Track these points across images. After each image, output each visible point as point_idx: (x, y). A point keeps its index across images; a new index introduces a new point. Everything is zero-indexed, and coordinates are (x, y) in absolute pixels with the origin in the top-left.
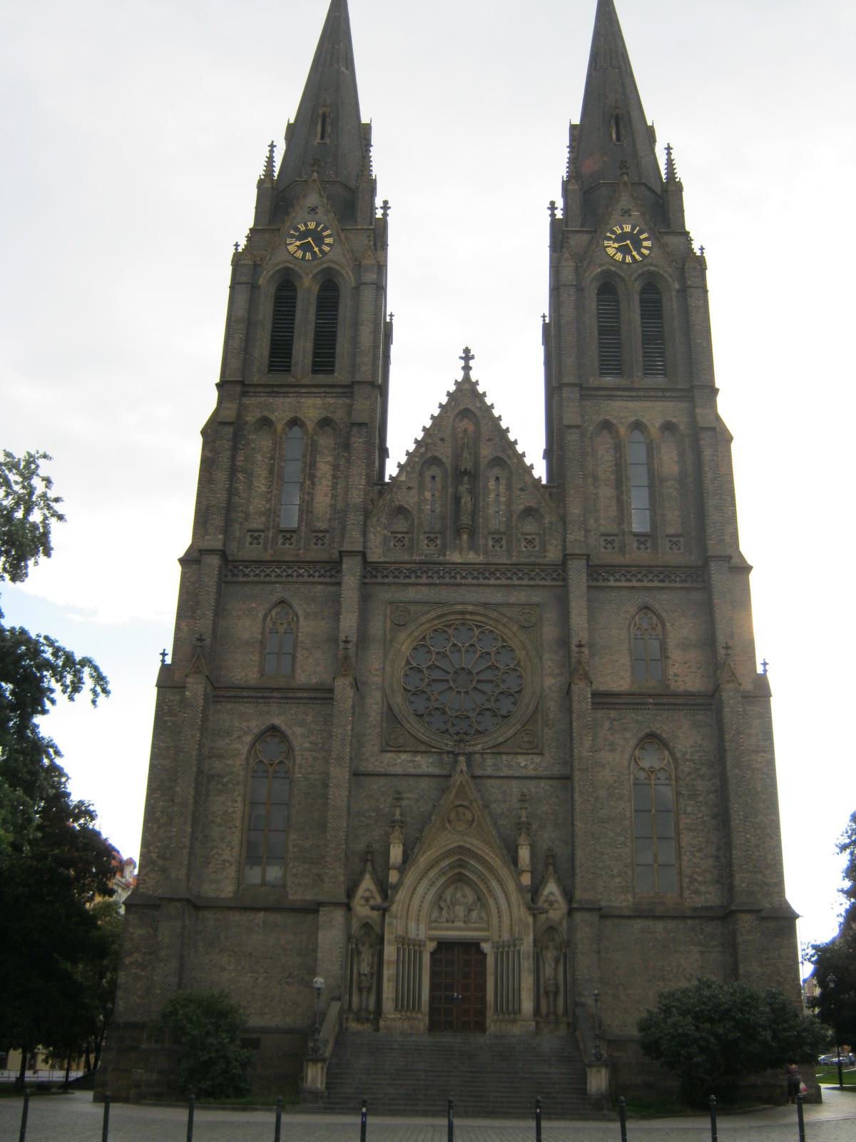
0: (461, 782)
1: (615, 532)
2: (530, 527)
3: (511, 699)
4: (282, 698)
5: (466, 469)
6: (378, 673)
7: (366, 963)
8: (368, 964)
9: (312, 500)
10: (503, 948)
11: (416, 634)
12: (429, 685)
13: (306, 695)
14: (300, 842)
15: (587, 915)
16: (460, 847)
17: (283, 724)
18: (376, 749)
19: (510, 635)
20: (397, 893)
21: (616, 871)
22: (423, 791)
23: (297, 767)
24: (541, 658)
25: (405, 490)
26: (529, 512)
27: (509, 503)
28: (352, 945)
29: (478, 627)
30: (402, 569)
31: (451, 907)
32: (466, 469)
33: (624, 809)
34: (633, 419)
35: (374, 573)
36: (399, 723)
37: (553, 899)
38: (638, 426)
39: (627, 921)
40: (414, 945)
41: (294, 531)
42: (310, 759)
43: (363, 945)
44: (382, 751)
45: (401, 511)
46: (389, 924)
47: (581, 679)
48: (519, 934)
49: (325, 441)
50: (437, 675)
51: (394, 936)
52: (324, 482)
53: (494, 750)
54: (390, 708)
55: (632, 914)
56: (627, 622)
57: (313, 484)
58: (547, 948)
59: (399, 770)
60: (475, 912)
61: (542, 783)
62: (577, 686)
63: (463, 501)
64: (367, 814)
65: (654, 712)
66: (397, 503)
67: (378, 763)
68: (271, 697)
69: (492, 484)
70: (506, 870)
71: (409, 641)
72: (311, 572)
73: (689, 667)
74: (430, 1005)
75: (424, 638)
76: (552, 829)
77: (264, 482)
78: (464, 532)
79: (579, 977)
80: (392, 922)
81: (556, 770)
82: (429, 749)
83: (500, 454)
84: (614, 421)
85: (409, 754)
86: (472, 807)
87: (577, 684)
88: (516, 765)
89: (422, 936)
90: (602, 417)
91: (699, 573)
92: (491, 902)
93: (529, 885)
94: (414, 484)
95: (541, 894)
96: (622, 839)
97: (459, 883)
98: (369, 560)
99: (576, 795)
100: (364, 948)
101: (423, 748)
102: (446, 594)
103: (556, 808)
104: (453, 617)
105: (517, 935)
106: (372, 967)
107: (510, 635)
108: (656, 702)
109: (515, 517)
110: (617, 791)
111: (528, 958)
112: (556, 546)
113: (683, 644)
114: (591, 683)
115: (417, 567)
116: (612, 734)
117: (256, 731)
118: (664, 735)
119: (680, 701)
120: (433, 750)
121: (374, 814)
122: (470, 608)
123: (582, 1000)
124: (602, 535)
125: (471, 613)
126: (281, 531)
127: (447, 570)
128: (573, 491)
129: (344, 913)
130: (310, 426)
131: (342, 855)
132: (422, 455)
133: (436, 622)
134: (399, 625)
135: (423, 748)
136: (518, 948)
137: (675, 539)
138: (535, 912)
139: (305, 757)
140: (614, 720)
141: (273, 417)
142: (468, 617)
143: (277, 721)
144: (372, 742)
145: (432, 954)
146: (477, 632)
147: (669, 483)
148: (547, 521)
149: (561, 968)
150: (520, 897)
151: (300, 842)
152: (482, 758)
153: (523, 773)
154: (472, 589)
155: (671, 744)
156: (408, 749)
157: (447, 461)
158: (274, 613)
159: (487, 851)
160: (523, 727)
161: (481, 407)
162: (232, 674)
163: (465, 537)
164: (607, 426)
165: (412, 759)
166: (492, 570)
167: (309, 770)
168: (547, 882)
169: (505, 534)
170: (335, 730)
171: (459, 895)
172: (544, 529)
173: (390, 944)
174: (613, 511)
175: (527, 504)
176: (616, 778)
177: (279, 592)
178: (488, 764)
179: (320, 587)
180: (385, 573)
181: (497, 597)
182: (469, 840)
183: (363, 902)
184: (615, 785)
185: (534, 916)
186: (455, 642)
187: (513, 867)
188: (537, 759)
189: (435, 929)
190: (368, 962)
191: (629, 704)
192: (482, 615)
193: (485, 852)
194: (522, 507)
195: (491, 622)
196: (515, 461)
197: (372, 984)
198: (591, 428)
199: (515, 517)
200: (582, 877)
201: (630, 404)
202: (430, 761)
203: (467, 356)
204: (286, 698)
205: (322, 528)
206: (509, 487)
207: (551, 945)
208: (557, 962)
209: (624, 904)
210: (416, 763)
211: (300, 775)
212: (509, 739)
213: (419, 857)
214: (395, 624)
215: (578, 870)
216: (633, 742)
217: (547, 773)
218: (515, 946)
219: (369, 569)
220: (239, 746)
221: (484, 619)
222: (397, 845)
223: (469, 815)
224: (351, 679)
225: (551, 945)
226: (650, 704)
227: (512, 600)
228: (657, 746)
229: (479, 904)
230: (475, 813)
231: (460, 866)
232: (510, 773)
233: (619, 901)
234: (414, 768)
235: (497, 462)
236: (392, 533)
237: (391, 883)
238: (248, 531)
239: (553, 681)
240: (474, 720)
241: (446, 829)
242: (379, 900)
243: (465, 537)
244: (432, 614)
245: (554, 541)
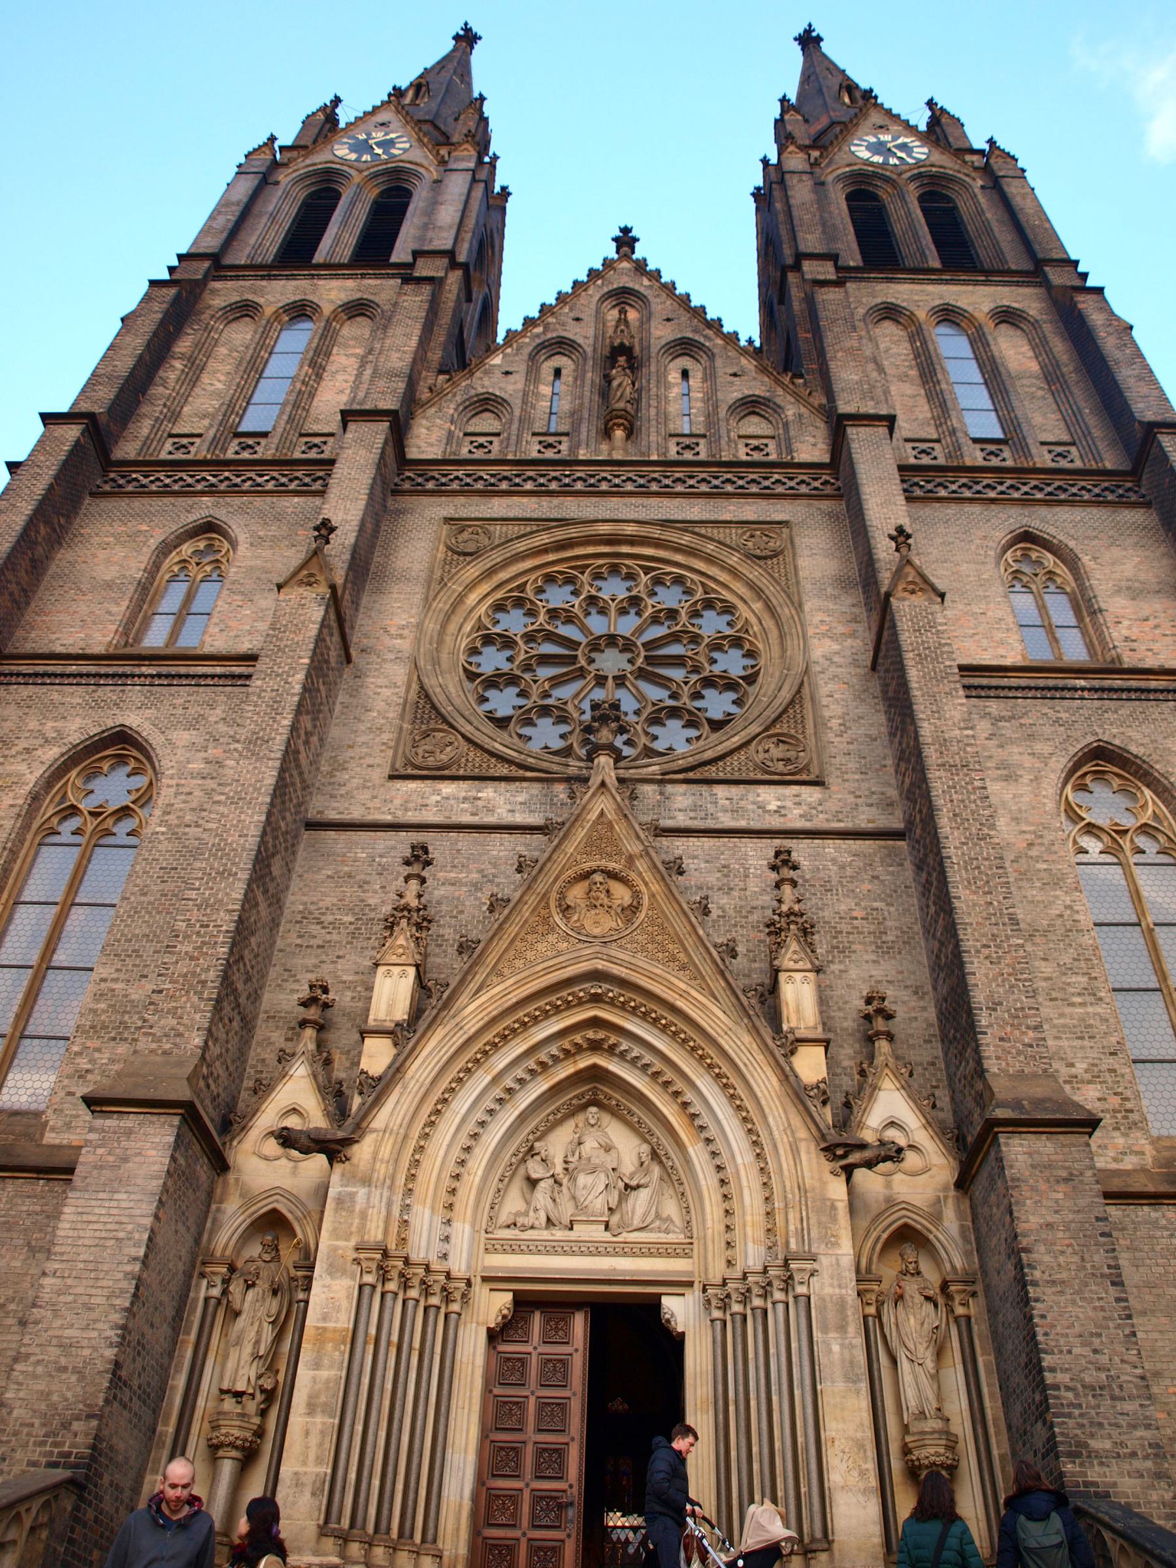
0: (602, 813)
1: (935, 436)
2: (754, 426)
3: (732, 696)
4: (159, 676)
5: (622, 345)
6: (406, 632)
7: (248, 1349)
8: (256, 1357)
9: (312, 395)
10: (745, 1299)
11: (503, 575)
12: (528, 668)
13: (219, 670)
14: (119, 986)
15: (1045, 1146)
16: (596, 976)
17: (147, 725)
18: (378, 775)
19: (723, 577)
20: (378, 1102)
21: (1080, 1067)
22: (495, 866)
23: (157, 812)
24: (801, 605)
25: (498, 374)
26: (751, 406)
27: (711, 399)
28: (210, 1286)
29: (647, 570)
30: (482, 474)
31: (565, 1181)
32: (622, 345)
33: (1067, 907)
34: (937, 302)
35: (420, 480)
36: (445, 721)
37: (902, 1142)
38: (948, 315)
39: (1145, 1212)
40: (427, 1291)
41: (265, 435)
42: (197, 793)
43: (249, 1286)
44: (392, 777)
45: (487, 403)
46: (340, 1201)
47: (913, 592)
48: (800, 1234)
49: (354, 331)
50: (548, 648)
51: (353, 1243)
52: (340, 377)
53: (691, 775)
54: (424, 693)
55: (1164, 1188)
56: (992, 553)
57: (319, 377)
58: (899, 1298)
59: (430, 817)
60: (643, 1195)
61: (831, 847)
62: (907, 603)
63: (615, 383)
64: (330, 918)
65: (1097, 703)
66: (481, 390)
67: (377, 803)
68: (133, 676)
69: (674, 376)
70: (747, 1038)
71: (485, 588)
72: (283, 480)
73: (1157, 627)
74: (475, 1532)
75: (522, 588)
76: (873, 957)
77: (222, 378)
78: (619, 425)
79: (1062, 1378)
80: (352, 1196)
81: (864, 819)
82: (521, 773)
83: (690, 335)
84: (904, 304)
85: (464, 785)
86: (633, 875)
87: (904, 599)
88: (750, 807)
89: (458, 1265)
90: (879, 300)
91: (1129, 485)
92: (697, 1153)
93: (824, 1081)
94: (521, 367)
95: (861, 1125)
96: (1085, 979)
97: (593, 1109)
98: (413, 453)
99: (944, 822)
100: (251, 1294)
101: (504, 770)
102: (571, 507)
103: (876, 905)
104: (591, 550)
105: (793, 1245)
106: (272, 1369)
107: (723, 577)
108: (1096, 684)
109: (723, 413)
110: (1045, 866)
111: (842, 1328)
112: (814, 445)
113: (1129, 588)
114: (942, 596)
115: (515, 470)
116: (1001, 746)
117: (75, 738)
118: (1133, 749)
119: (1153, 684)
120: (529, 774)
121: (350, 919)
122: (630, 529)
123: (1094, 1473)
124: (907, 440)
125: (632, 541)
126: (237, 435)
127: (579, 474)
128: (839, 355)
129: (172, 1139)
130: (327, 309)
131: (212, 974)
132: (538, 336)
133: (551, 557)
134: (466, 554)
135: (504, 770)
136: (801, 1289)
137: (1060, 449)
138: (855, 1157)
139: (187, 790)
140: (1001, 719)
141: (261, 301)
142: (625, 549)
143: (133, 720)
144: (369, 761)
145: (494, 1336)
146: (644, 578)
147: (1025, 382)
148: (790, 413)
149: (955, 1376)
150: (796, 1121)
151: (119, 986)
152: (661, 793)
153: (776, 823)
154: (633, 500)
155: (1157, 767)
156: (461, 772)
157: (587, 344)
158: (187, 549)
159: (683, 986)
160: (766, 729)
161: (650, 287)
162: (53, 637)
163: (619, 433)
164: (890, 312)
165: (474, 793)
166: (678, 475)
167: (188, 818)
168: (875, 1088)
169: (704, 436)
170: (259, 683)
171: (590, 1145)
172: (786, 425)
173: (334, 1270)
174: (924, 410)
175: (747, 392)
176: (1028, 836)
177: (205, 508)
178: (678, 806)
179: (296, 499)
180: (443, 480)
181: (695, 510)
182: (614, 951)
183: (272, 1147)
184: (1034, 852)
185: (849, 1170)
186: (594, 592)
187: (767, 1032)
188: (811, 794)
189: (512, 1248)
190: (257, 1343)
191: (1030, 688)
192: (658, 544)
193: (671, 987)
194: (737, 395)
195: (679, 558)
196: (719, 342)
197: (260, 1433)
198: (861, 311)
199: (723, 413)
200: (1001, 1039)
201: (930, 288)
202: (520, 799)
203: (626, 240)
204: (167, 676)
205: (325, 431)
206: (710, 375)
207: (911, 1287)
208: (939, 1354)
209: (1129, 1163)
210: (480, 803)
211: (163, 829)
212: (731, 753)
213: (463, 999)
214: (455, 552)
215: (983, 1020)
216: (1061, 763)
217: (842, 825)
218: (788, 1282)
219: (408, 474)
220: (23, 768)
221: (661, 553)
222: (396, 970)
223: (621, 894)
224: (323, 590)
225: (911, 1287)
226: (1083, 689)
227: (727, 517)
228: (1116, 782)
229: (656, 1170)
230: (643, 888)
231: (595, 1046)
232: (742, 824)
233: (1111, 1153)
234: (473, 814)
235: (684, 347)
236: (466, 434)
237: (362, 1072)
238: (171, 436)
239: (836, 647)
240: (639, 728)
241: (552, 929)
242: (316, 1118)
243: (619, 433)
244: (544, 538)
245: (812, 440)
